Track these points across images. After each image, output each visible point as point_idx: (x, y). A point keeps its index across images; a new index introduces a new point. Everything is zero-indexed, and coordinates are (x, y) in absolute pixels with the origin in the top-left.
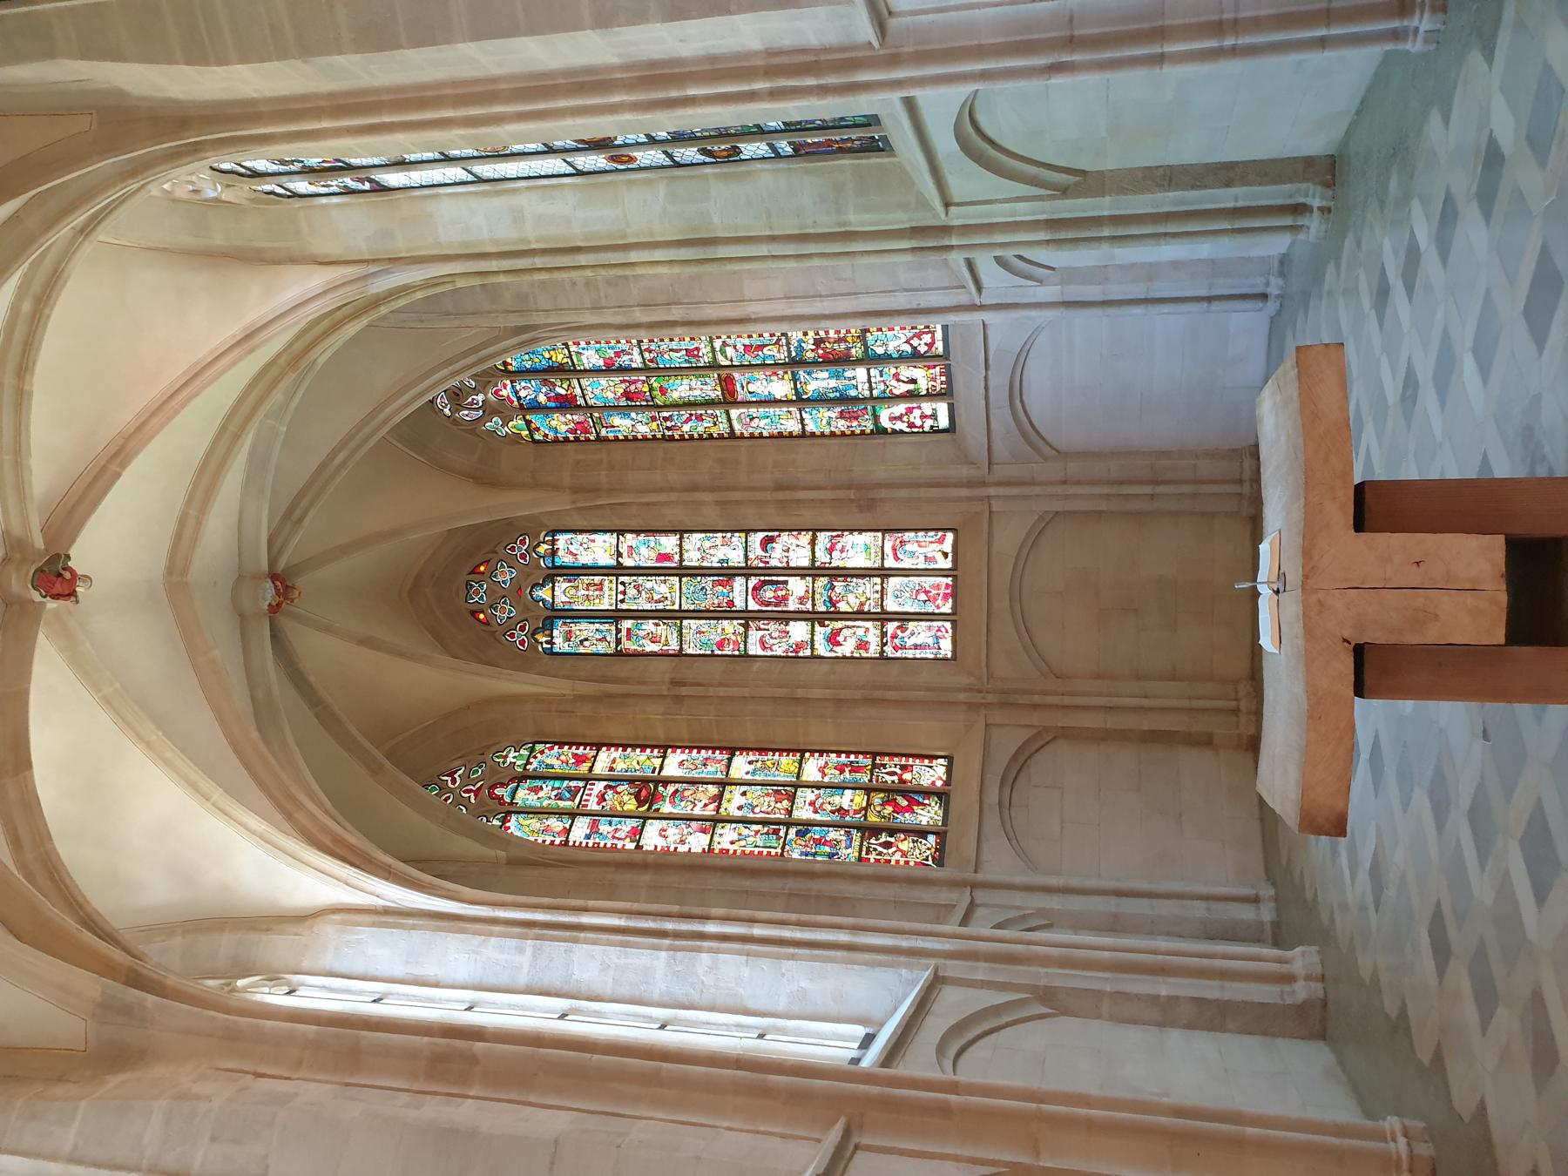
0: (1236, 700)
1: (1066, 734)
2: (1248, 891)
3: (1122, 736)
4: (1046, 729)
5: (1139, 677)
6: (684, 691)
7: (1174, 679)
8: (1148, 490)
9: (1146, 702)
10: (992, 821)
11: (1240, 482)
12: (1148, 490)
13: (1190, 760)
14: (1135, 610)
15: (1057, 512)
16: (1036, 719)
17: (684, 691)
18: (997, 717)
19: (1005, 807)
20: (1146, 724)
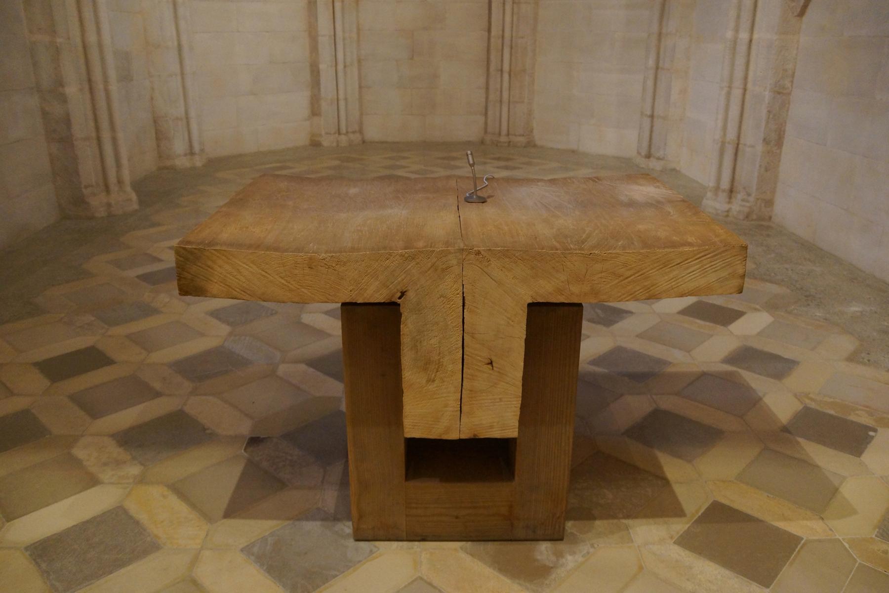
0: (347, 132)
3: (314, 48)
5: (359, 61)
7: (360, 87)
8: (506, 67)
9: (340, 67)
11: (508, 135)
12: (506, 67)
13: (300, 100)
14: (412, 58)
20: (325, 67)
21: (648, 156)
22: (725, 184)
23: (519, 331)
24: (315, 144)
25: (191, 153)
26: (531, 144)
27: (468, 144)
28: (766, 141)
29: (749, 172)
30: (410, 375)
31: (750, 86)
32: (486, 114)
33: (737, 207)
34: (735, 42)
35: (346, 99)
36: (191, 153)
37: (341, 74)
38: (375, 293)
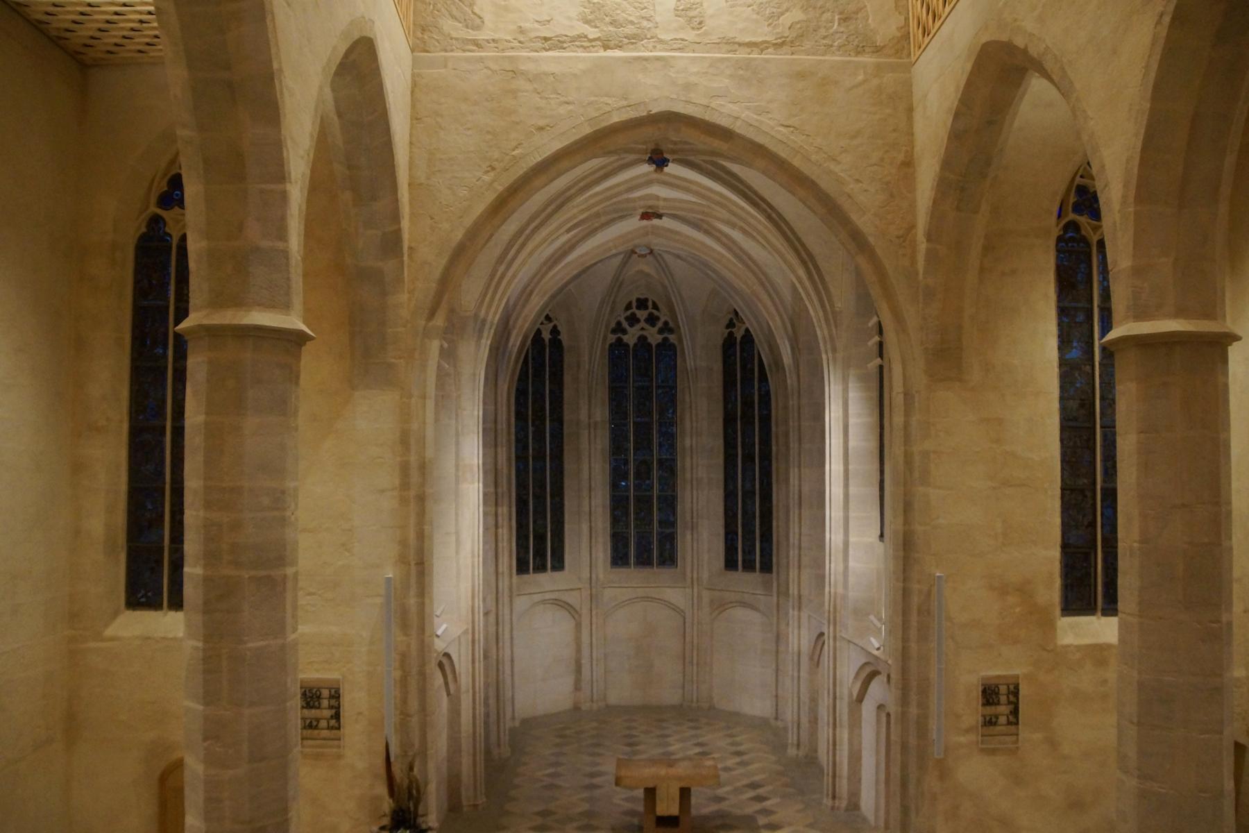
1: (578, 626)
2: (516, 715)
3: (579, 650)
4: (580, 616)
6: (592, 431)
7: (605, 672)
8: (695, 662)
10: (537, 598)
11: (698, 701)
12: (695, 662)
13: (569, 681)
15: (685, 619)
16: (585, 611)
17: (592, 431)
18: (586, 593)
19: (544, 602)
21: (776, 719)
22: (795, 742)
23: (678, 793)
24: (576, 708)
25: (513, 718)
26: (712, 708)
27: (673, 707)
28: (810, 722)
29: (804, 736)
30: (658, 802)
31: (801, 696)
32: (683, 687)
33: (801, 753)
34: (793, 676)
35: (597, 681)
36: (513, 718)
37: (594, 666)
38: (651, 785)
